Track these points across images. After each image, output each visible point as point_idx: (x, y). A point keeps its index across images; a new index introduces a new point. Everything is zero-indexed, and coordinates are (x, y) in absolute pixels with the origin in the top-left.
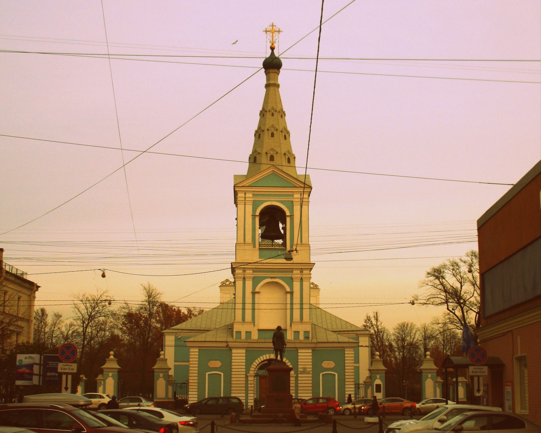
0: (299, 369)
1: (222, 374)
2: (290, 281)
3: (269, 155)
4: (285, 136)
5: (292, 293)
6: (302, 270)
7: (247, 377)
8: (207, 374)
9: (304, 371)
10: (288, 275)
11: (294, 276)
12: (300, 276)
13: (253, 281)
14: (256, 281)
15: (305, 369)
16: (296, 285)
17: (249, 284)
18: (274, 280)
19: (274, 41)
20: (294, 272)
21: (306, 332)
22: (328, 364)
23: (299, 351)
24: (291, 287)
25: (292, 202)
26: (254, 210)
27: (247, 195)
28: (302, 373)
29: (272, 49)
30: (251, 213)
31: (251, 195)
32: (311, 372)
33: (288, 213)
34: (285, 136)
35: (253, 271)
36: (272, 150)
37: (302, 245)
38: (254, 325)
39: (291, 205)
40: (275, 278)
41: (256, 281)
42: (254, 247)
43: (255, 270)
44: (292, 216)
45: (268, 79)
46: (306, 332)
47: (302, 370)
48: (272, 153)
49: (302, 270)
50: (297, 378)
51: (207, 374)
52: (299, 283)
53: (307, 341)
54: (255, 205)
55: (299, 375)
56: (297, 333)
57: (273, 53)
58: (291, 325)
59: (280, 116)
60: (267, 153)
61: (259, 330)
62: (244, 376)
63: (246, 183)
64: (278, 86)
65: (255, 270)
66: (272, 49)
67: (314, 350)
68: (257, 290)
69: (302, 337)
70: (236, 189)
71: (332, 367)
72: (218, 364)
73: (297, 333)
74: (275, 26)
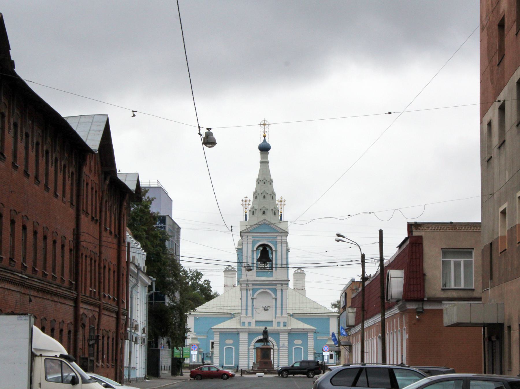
0: (280, 345)
1: (234, 348)
2: (275, 291)
3: (262, 211)
4: (272, 197)
5: (276, 299)
6: (282, 284)
7: (249, 349)
8: (225, 347)
9: (283, 346)
10: (273, 287)
11: (277, 288)
12: (281, 288)
14: (254, 291)
15: (284, 345)
16: (279, 293)
17: (250, 293)
18: (265, 290)
20: (278, 285)
21: (285, 322)
22: (298, 342)
23: (280, 334)
25: (276, 242)
26: (253, 247)
27: (249, 237)
28: (282, 347)
30: (251, 249)
31: (251, 238)
32: (287, 347)
33: (274, 249)
34: (272, 197)
35: (253, 285)
36: (264, 207)
38: (253, 318)
39: (276, 244)
41: (254, 291)
43: (253, 285)
44: (276, 251)
45: (262, 158)
46: (285, 322)
47: (282, 345)
48: (264, 209)
49: (282, 284)
50: (278, 350)
51: (225, 347)
52: (280, 292)
53: (285, 328)
54: (253, 243)
55: (280, 349)
56: (279, 323)
57: (265, 140)
58: (275, 318)
60: (261, 209)
61: (256, 321)
62: (247, 349)
65: (253, 285)
67: (289, 333)
68: (255, 296)
69: (282, 324)
70: (242, 234)
71: (300, 343)
72: (230, 341)
73: (279, 323)
74: (266, 121)
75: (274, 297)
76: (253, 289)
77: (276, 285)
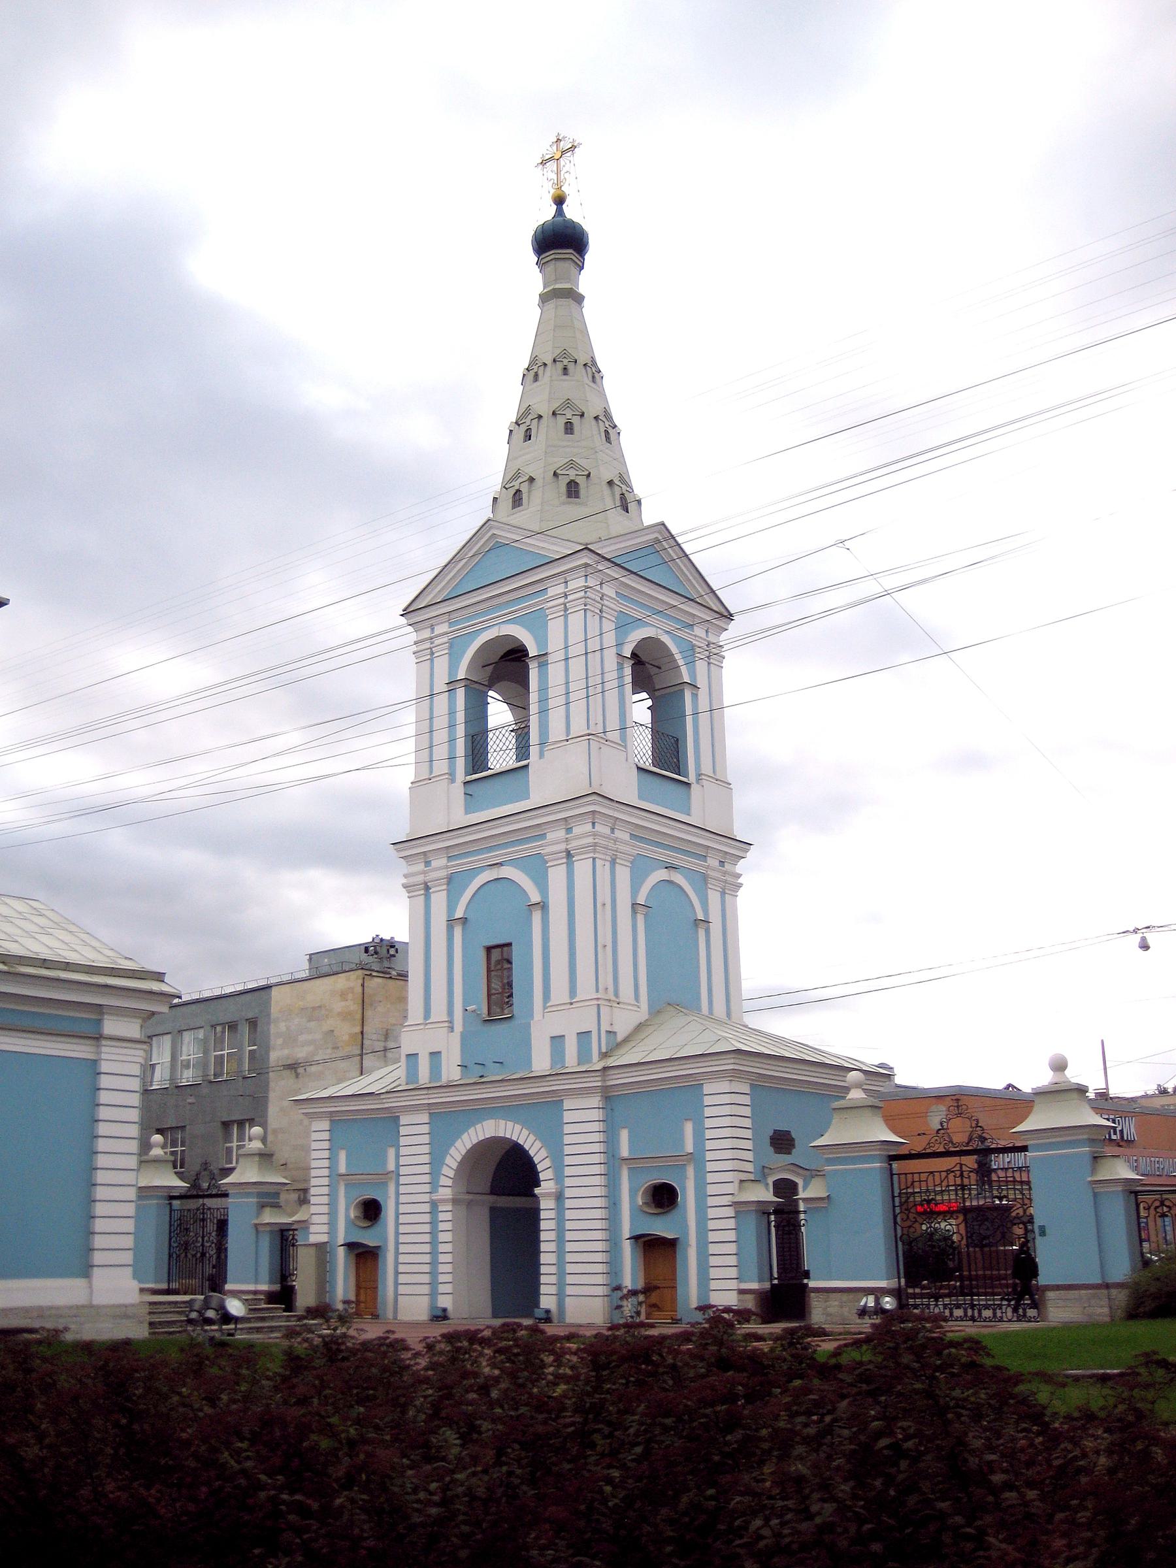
5: (543, 906)
13: (448, 890)
16: (557, 876)
19: (562, 177)
24: (543, 887)
29: (560, 201)
37: (570, 742)
40: (501, 864)
42: (452, 779)
43: (451, 853)
44: (542, 657)
56: (557, 1041)
57: (560, 212)
59: (591, 379)
63: (432, 595)
64: (579, 299)
66: (560, 201)
75: (535, 897)
76: (450, 879)
77: (543, 836)
